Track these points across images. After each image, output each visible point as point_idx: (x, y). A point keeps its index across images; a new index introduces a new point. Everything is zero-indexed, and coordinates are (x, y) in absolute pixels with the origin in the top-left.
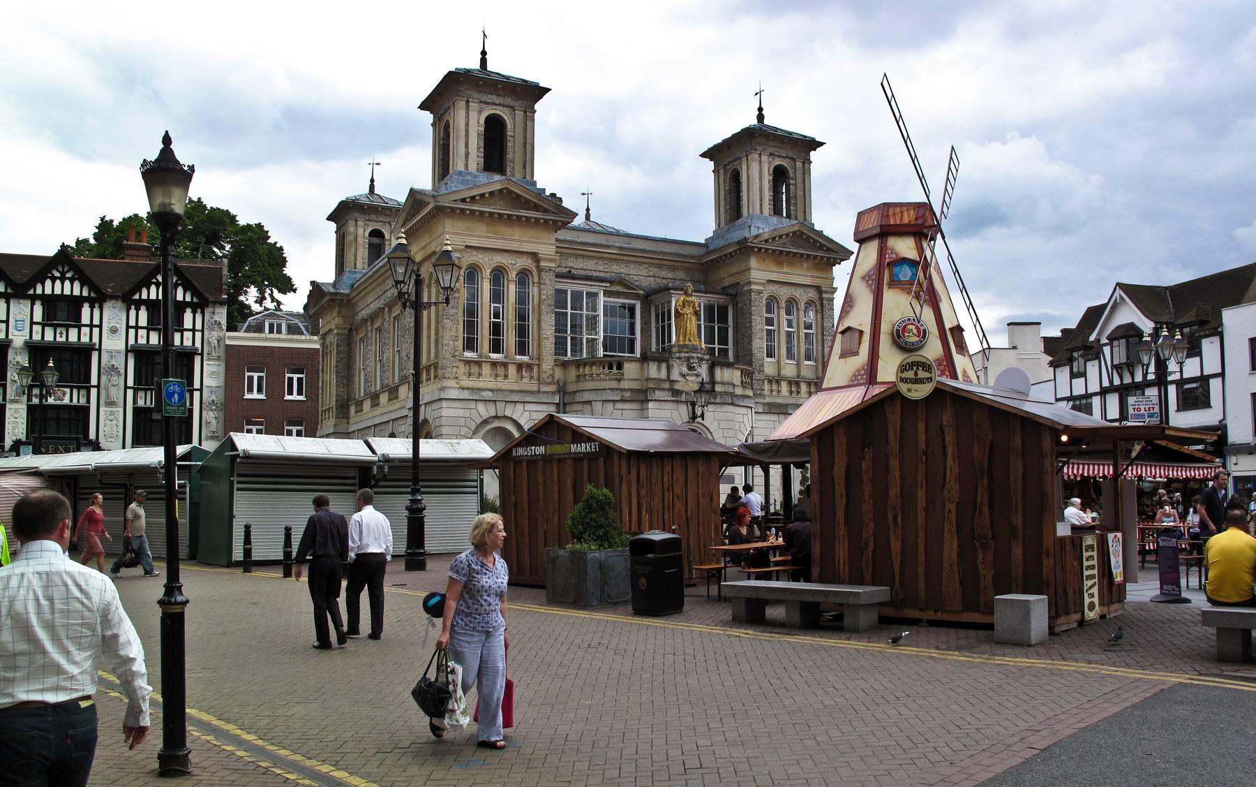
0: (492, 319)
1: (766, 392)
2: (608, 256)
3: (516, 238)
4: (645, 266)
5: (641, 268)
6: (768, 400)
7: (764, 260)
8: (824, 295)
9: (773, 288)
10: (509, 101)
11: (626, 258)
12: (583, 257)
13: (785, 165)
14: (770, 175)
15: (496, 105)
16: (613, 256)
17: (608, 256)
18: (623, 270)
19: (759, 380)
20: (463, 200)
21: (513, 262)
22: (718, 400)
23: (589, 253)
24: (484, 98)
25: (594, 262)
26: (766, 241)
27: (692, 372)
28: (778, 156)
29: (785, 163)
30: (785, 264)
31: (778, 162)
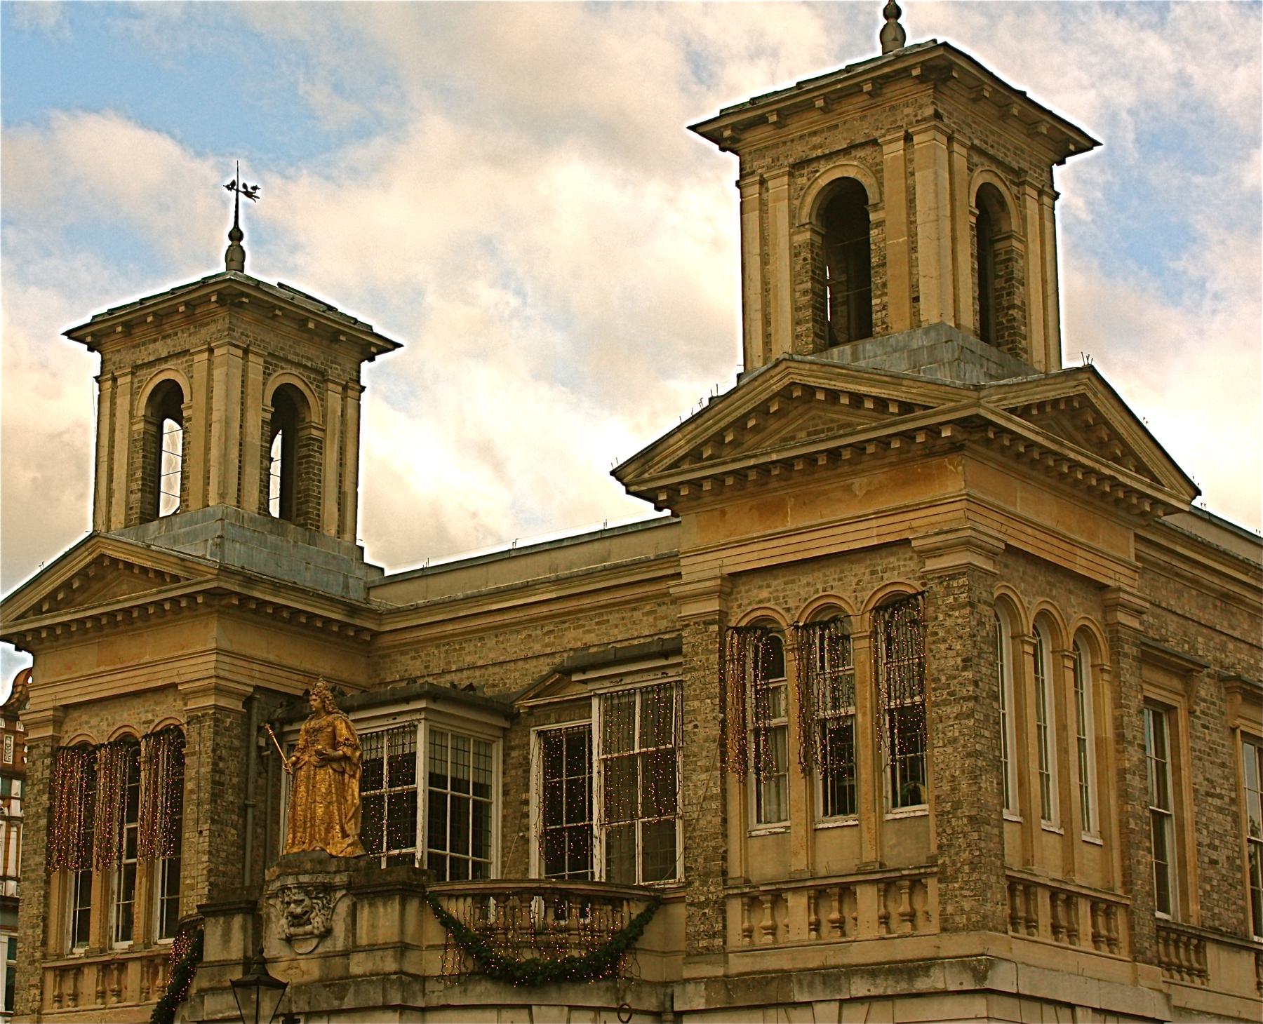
0: (125, 861)
1: (735, 938)
2: (544, 610)
3: (147, 658)
4: (648, 608)
5: (637, 615)
6: (737, 965)
7: (723, 513)
8: (931, 565)
9: (765, 594)
10: (183, 340)
11: (587, 602)
12: (496, 629)
13: (851, 173)
14: (795, 227)
15: (166, 359)
16: (555, 607)
17: (544, 610)
18: (591, 638)
19: (706, 903)
20: (37, 609)
21: (150, 717)
22: (349, 1003)
23: (499, 618)
24: (144, 356)
25: (525, 633)
26: (695, 455)
27: (300, 930)
28: (828, 157)
29: (850, 169)
30: (791, 502)
31: (828, 174)
